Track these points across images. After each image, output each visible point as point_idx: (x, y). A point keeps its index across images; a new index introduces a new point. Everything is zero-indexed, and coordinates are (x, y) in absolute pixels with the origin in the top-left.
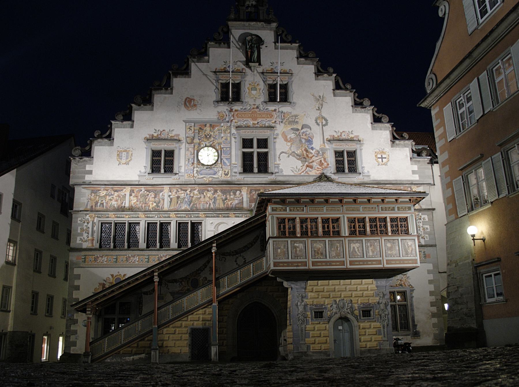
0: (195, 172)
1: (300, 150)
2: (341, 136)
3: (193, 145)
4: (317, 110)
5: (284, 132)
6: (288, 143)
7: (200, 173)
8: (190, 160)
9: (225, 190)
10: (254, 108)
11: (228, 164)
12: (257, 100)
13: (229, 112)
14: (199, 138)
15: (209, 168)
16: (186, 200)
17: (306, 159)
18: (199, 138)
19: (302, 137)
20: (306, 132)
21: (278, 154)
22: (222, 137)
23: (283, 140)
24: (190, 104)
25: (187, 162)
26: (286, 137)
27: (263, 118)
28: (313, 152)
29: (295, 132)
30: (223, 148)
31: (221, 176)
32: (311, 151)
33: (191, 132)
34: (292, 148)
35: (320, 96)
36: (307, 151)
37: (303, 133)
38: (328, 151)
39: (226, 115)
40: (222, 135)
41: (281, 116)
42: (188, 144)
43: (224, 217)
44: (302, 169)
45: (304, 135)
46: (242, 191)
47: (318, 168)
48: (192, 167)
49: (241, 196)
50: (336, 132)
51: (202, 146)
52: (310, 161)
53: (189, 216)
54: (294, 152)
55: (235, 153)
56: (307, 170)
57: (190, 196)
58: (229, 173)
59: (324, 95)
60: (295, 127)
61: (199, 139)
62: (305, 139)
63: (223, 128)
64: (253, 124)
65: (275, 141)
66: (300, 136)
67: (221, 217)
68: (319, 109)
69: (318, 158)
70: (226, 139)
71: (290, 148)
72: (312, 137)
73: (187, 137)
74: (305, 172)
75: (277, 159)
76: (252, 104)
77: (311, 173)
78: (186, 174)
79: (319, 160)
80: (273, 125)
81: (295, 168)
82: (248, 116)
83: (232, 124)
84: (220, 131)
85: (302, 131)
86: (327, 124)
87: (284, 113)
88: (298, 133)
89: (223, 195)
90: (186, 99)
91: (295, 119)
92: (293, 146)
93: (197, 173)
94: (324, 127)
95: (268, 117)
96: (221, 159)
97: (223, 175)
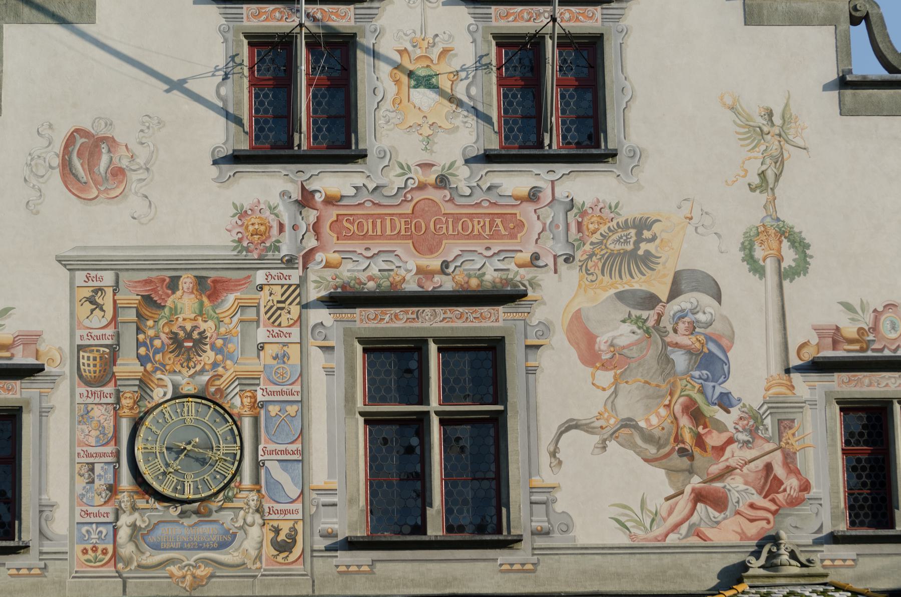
0: (124, 533)
1: (663, 412)
2: (874, 329)
3: (109, 389)
4: (753, 190)
5: (577, 316)
6: (599, 372)
7: (152, 538)
8: (98, 469)
10: (422, 187)
11: (293, 491)
12: (441, 139)
13: (294, 208)
14: (142, 351)
15: (197, 512)
17: (692, 457)
18: (142, 351)
19: (671, 337)
20: (694, 312)
21: (547, 435)
22: (261, 347)
23: (574, 354)
24: (91, 167)
25: (81, 483)
26: (591, 339)
27: (470, 236)
28: (729, 419)
29: (635, 313)
30: (263, 405)
31: (259, 557)
32: (720, 414)
33: (98, 320)
34: (620, 402)
35: (770, 114)
36: (695, 414)
37: (681, 316)
38: (808, 412)
39: (281, 227)
40: (262, 335)
41: (567, 226)
42: (88, 383)
44: (670, 512)
45: (681, 327)
47: (752, 506)
48: (108, 509)
50: (848, 307)
51: (158, 394)
52: (715, 469)
54: (629, 424)
55: (329, 431)
56: (695, 518)
58: (299, 538)
59: (793, 110)
60: (639, 283)
62: (689, 351)
63: (264, 296)
64: (420, 271)
65: (530, 363)
66: (663, 333)
68: (763, 184)
69: (754, 453)
70: (282, 358)
71: (611, 402)
72: (724, 342)
73: (80, 348)
74: (684, 529)
75: (545, 459)
76: (412, 162)
77: (716, 536)
78: (78, 548)
79: (760, 464)
80: (525, 274)
81: (639, 512)
82: (393, 228)
83: (312, 276)
84: (251, 314)
85: (675, 307)
86: (801, 268)
87: (583, 213)
88: (650, 316)
90: (70, 141)
91: (639, 239)
92: (623, 386)
93: (132, 538)
94: (786, 283)
95: (495, 235)
96: (258, 465)
97: (269, 550)
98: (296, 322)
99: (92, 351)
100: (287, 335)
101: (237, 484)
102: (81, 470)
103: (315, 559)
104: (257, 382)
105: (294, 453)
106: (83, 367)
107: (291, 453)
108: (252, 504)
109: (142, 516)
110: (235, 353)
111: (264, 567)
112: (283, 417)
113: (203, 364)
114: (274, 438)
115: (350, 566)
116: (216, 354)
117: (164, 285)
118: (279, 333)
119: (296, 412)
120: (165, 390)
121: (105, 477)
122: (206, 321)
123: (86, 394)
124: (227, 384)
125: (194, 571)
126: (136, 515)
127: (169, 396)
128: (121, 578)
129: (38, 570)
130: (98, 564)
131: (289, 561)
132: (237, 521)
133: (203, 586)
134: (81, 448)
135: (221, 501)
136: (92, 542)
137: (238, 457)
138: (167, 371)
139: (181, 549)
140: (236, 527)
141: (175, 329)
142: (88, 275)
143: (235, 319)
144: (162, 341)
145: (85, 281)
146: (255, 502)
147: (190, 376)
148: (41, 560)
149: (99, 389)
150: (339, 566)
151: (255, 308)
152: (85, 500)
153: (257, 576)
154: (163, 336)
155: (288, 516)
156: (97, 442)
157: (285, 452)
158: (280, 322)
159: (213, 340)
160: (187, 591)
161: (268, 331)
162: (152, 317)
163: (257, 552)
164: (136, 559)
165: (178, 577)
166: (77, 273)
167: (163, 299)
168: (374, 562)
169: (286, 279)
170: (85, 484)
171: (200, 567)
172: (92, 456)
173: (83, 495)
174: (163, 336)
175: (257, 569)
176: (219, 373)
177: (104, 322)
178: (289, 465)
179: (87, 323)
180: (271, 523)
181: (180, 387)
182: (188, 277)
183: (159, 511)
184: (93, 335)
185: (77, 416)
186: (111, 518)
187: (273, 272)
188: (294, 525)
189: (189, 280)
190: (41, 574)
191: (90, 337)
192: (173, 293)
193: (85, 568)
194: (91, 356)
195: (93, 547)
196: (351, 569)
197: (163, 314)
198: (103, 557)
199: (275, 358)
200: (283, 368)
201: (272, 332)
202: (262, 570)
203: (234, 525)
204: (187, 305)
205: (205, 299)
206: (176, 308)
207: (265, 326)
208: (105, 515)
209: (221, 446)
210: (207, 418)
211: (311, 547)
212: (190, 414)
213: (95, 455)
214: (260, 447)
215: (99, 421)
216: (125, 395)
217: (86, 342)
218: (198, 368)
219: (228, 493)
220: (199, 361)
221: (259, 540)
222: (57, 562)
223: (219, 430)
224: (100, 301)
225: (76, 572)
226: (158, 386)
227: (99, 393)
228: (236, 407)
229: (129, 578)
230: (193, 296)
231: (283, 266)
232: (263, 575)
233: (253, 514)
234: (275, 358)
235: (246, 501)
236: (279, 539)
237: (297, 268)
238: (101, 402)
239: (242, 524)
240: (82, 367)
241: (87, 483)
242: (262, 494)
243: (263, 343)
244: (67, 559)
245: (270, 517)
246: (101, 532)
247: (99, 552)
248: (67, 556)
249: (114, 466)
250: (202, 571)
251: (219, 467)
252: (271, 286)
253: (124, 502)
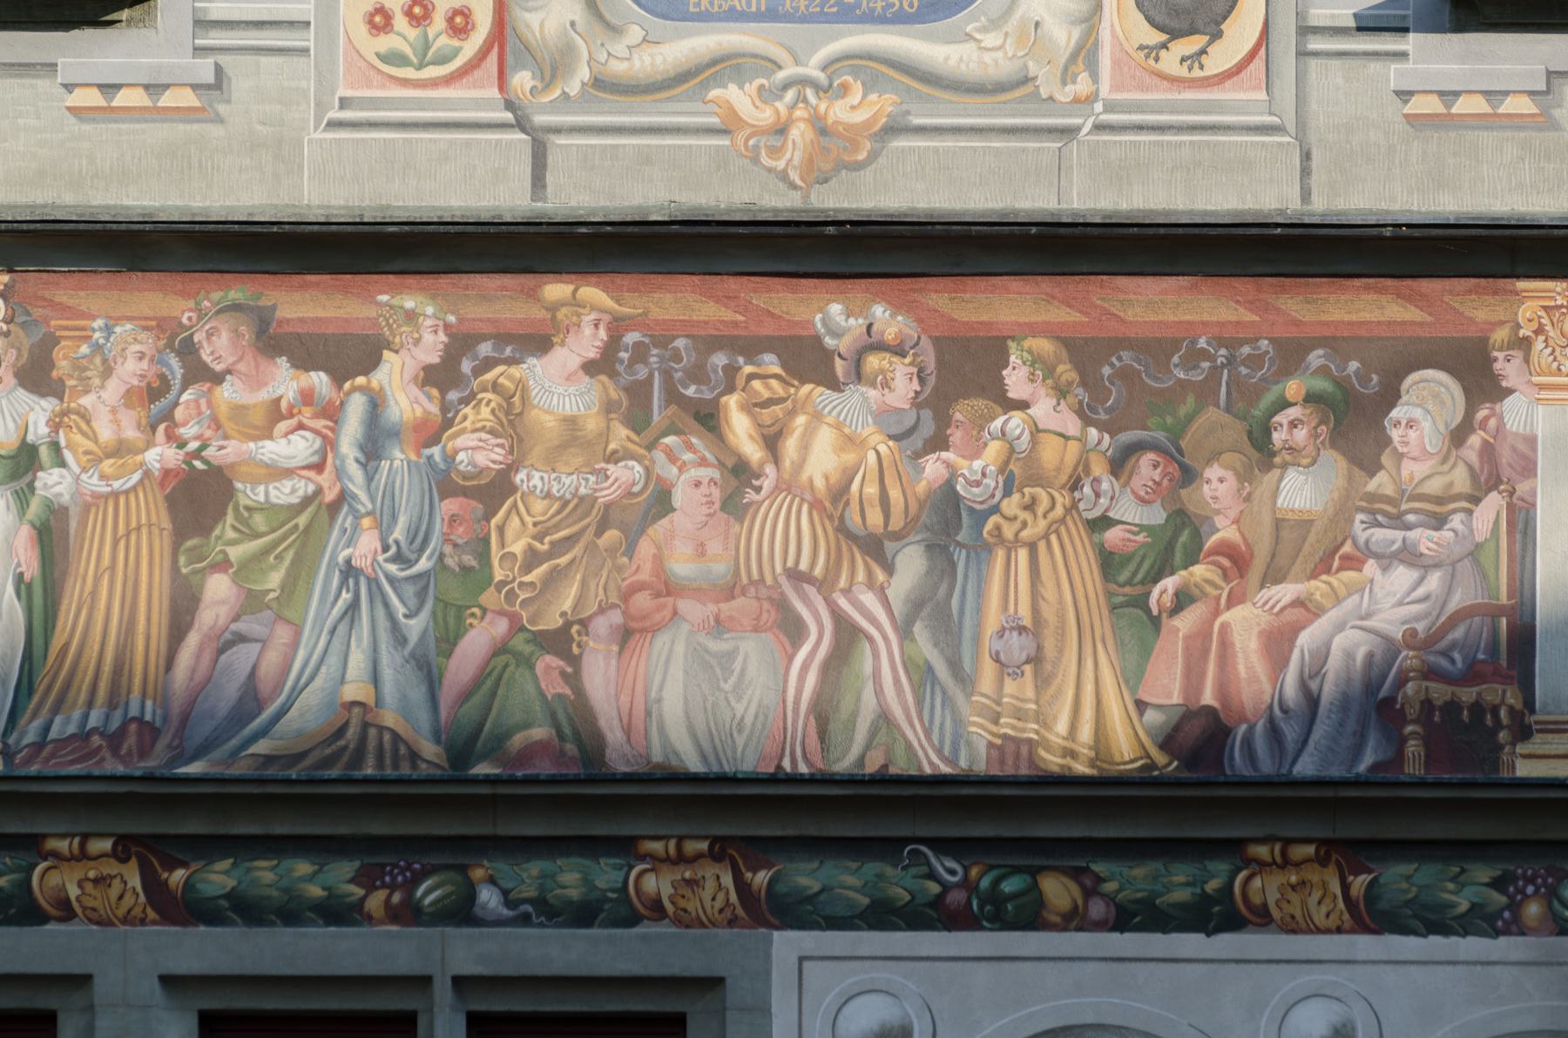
9: (1157, 348)
16: (365, 550)
31: (1085, 54)
43: (1124, 919)
46: (1508, 369)
49: (1488, 478)
53: (429, 892)
57: (445, 483)
67: (1074, 920)
89: (1119, 464)
103: (1313, 63)
111: (1105, 91)
115: (1456, 94)
125: (822, 107)
128: (524, 130)
129: (189, 91)
131: (1207, 72)
133: (858, 166)
139: (771, 15)
148: (199, 51)
150: (1411, 93)
153: (1078, 129)
160: (794, 186)
163: (1076, 34)
165: (759, 132)
168: (1556, 82)
171: (845, 90)
175: (1076, 100)
190: (202, 109)
193: (383, 86)
196: (1461, 106)
198: (455, 43)
202: (1098, 107)
211: (1300, 15)
222: (264, 60)
225: (344, 103)
229: (558, 130)
232: (1099, 128)
244: (305, 51)
247: (439, 22)
248: (309, 40)
250: (853, 108)
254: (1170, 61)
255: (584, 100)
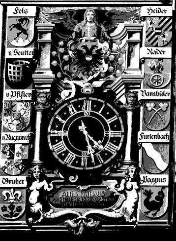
0: (34, 197)
3: (29, 91)
8: (17, 149)
11: (162, 165)
14: (55, 63)
31: (134, 214)
33: (21, 42)
48: (24, 178)
51: (64, 94)
61: (54, 69)
63: (145, 25)
93: (40, 200)
96: (136, 147)
97: (141, 208)
98: (168, 43)
99: (17, 63)
100: (162, 53)
101: (120, 160)
102: (4, 149)
104: (139, 86)
105: (164, 138)
106: (10, 75)
107: (162, 137)
108: (131, 174)
109: (49, 182)
110: (123, 65)
111: (138, 220)
112: (157, 111)
113: (99, 72)
114: (149, 127)
116: (109, 66)
117: (73, 17)
118: (156, 51)
119: (167, 108)
120: (70, 91)
121: (22, 155)
122: (102, 43)
123: (11, 94)
124: (117, 86)
125: (86, 223)
126: (44, 182)
127: (73, 95)
130: (13, 218)
131: (158, 216)
132: (119, 187)
134: (5, 133)
135: (108, 172)
136: (9, 202)
137: (122, 140)
138: (72, 77)
140: (119, 192)
141: (80, 48)
142: (17, 9)
143: (124, 41)
144: (70, 56)
145: (14, 13)
146: (133, 173)
147: (89, 82)
149: (21, 90)
151: (139, 34)
152: (6, 171)
154: (70, 53)
155: (158, 184)
156: (17, 128)
157: (158, 137)
158: (158, 43)
159: (107, 55)
161: (148, 49)
162: (64, 39)
163: (133, 209)
164: (42, 215)
166: (9, 7)
167: (71, 26)
169: (162, 13)
170: (7, 160)
171: (90, 221)
172: (13, 139)
173: (5, 168)
174: (70, 53)
176: (111, 79)
177: (27, 42)
178: (160, 146)
179: (14, 43)
180: (145, 188)
181: (82, 89)
182: (90, 11)
183: (62, 179)
184: (18, 52)
185: (3, 110)
186: (25, 184)
187: (154, 8)
188: (162, 190)
189: (91, 13)
191: (16, 53)
192: (79, 22)
194: (16, 66)
195: (10, 206)
197: (71, 37)
199: (153, 69)
200: (158, 76)
201: (151, 51)
202: (137, 223)
203: (117, 190)
204: (89, 31)
205: (102, 26)
206: (81, 32)
207: (146, 46)
208: (21, 182)
209: (110, 132)
210: (100, 112)
212: (88, 109)
213: (15, 138)
214: (139, 133)
215: (20, 114)
216: (40, 95)
217: (13, 57)
218: (95, 75)
219: (114, 166)
220: (96, 71)
221: (135, 200)
223: (109, 120)
224: (25, 27)
226: (65, 88)
227: (21, 93)
228: (122, 104)
230: (93, 24)
231: (161, 3)
233: (131, 181)
234: (153, 69)
235: (126, 172)
236: (150, 200)
237: (171, 5)
238: (22, 100)
239: (123, 189)
240: (9, 74)
241: (8, 159)
242: (139, 168)
243: (143, 58)
245: (144, 184)
246: (17, 195)
247: (15, 209)
249: (30, 147)
251: (107, 147)
252: (152, 18)
253: (35, 172)
254: (150, 215)
255: (42, 223)
